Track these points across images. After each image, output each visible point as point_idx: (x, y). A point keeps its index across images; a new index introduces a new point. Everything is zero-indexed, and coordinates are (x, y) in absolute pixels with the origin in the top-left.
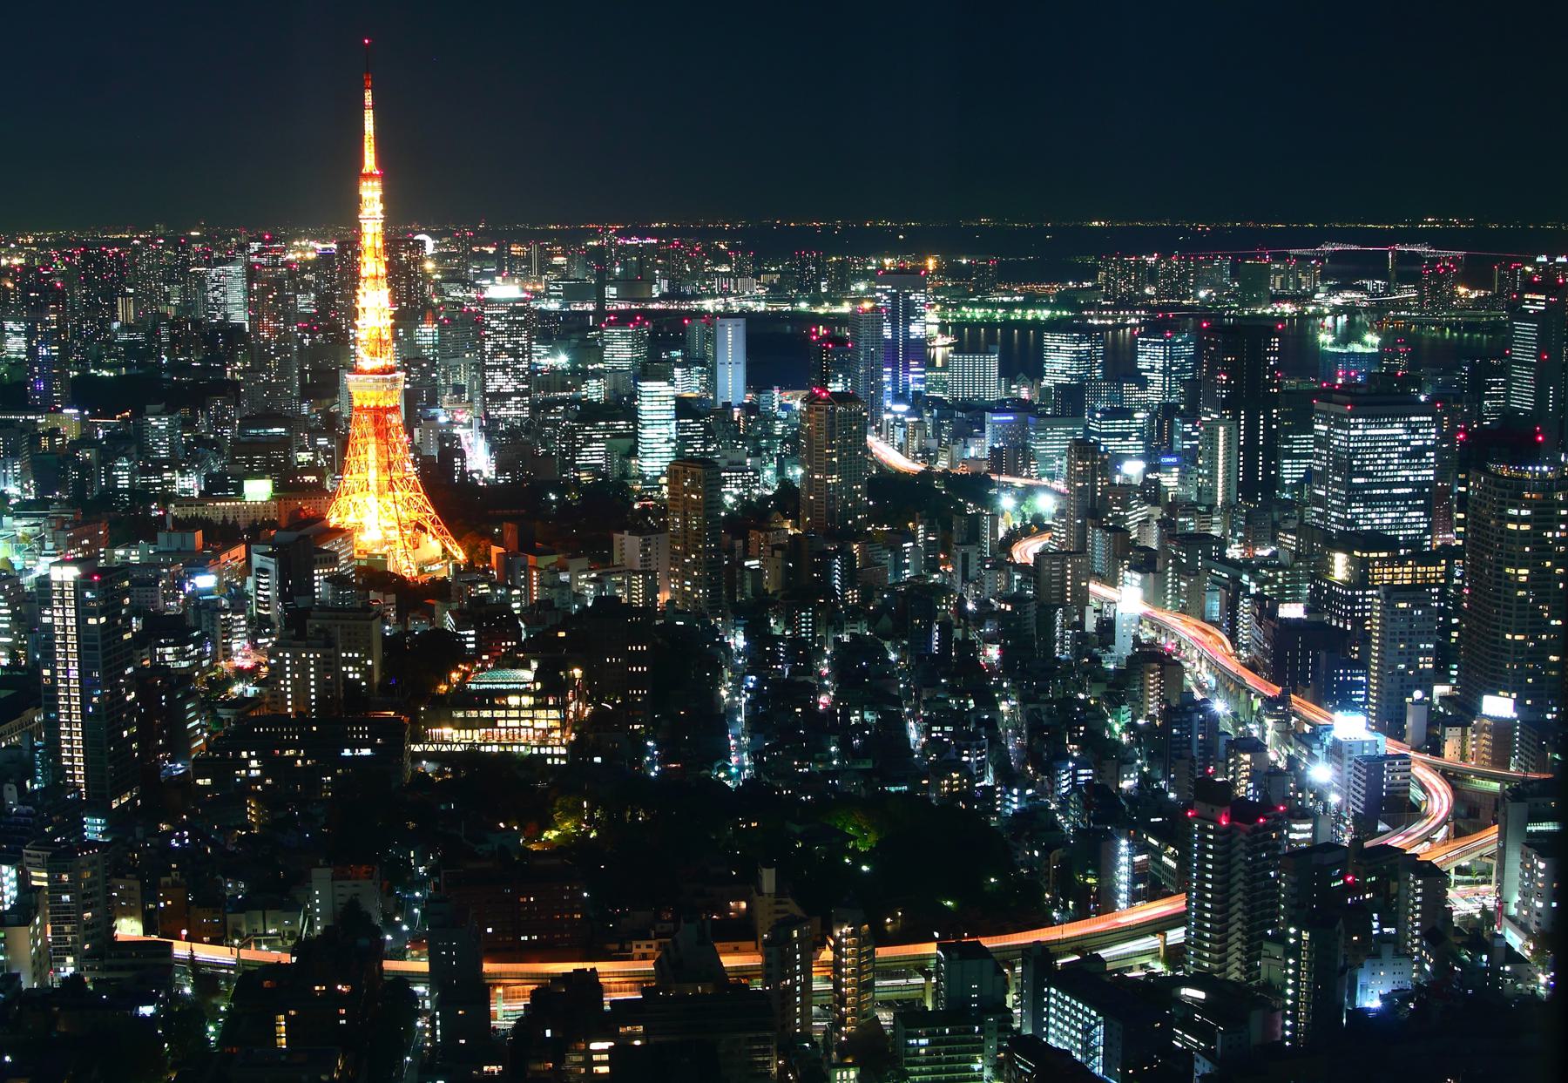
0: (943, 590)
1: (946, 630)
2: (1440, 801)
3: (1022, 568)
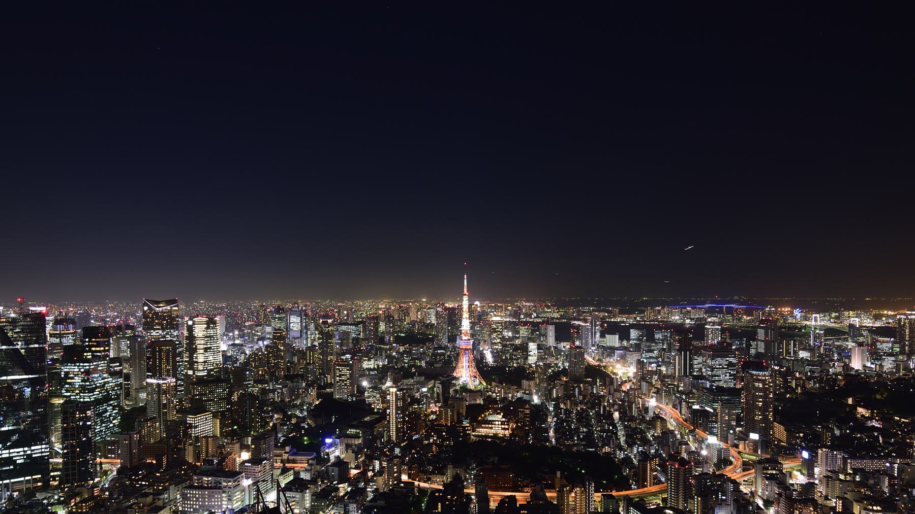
0: (603, 397)
1: (604, 407)
2: (737, 463)
3: (624, 392)
